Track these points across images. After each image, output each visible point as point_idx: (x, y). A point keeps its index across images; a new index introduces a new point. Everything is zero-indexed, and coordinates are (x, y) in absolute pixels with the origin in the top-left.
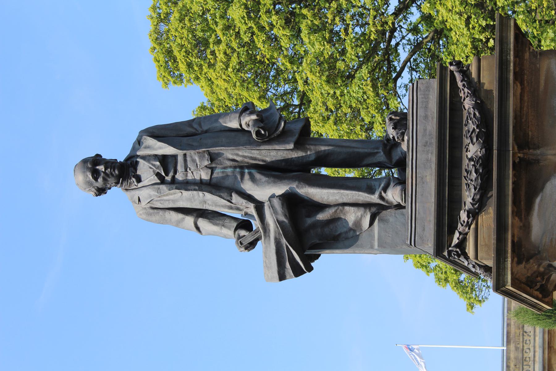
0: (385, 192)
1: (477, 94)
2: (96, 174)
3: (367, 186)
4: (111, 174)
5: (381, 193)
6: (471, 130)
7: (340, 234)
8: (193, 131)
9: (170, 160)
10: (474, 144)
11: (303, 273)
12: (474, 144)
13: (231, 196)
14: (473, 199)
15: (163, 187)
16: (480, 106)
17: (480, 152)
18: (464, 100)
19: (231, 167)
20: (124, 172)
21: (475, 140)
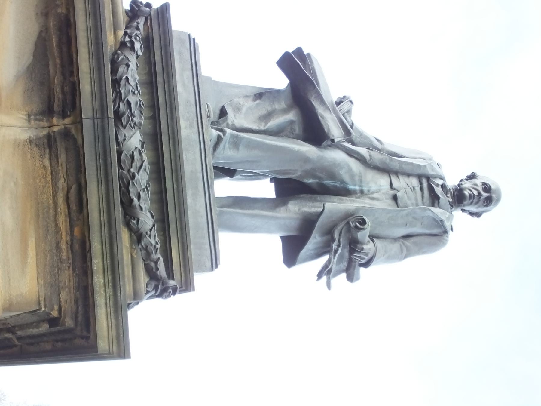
0: (219, 136)
1: (135, 238)
2: (487, 188)
3: (238, 149)
4: (471, 191)
5: (224, 134)
6: (141, 171)
7: (255, 100)
8: (406, 242)
9: (428, 202)
10: (136, 148)
11: (293, 52)
12: (136, 148)
13: (370, 156)
14: (128, 65)
15: (431, 172)
16: (129, 210)
17: (125, 136)
18: (154, 226)
19: (374, 193)
20: (459, 198)
21: (136, 154)
